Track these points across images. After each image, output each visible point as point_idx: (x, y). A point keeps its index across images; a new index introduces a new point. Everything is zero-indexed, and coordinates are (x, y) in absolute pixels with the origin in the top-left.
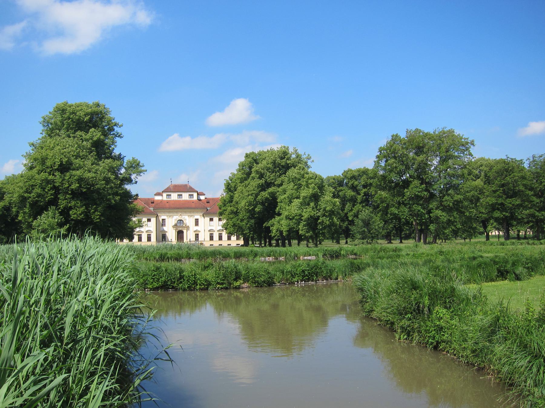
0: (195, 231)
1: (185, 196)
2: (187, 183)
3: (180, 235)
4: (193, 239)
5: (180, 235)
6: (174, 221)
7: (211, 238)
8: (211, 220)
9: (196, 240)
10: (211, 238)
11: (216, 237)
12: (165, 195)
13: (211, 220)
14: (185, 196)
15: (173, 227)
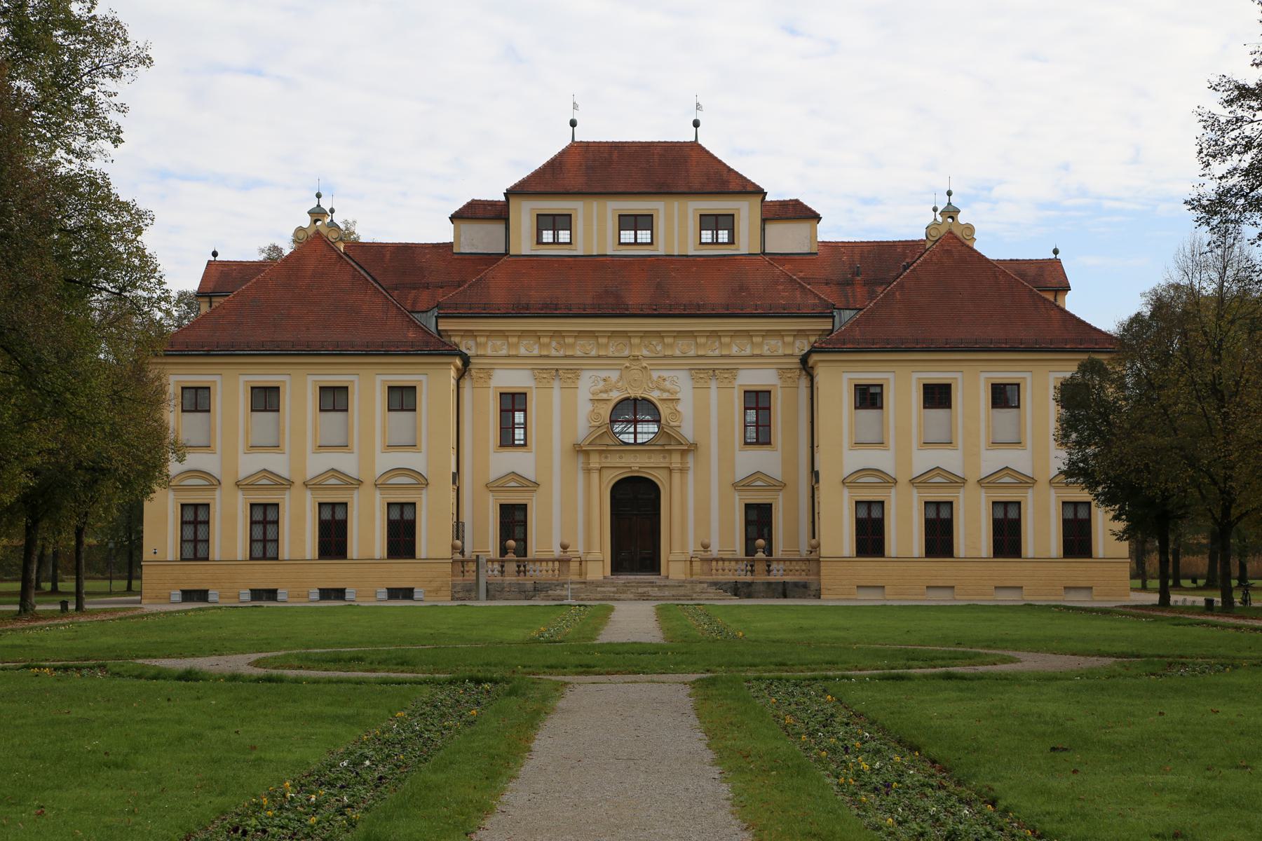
0: (742, 485)
1: (677, 228)
2: (687, 136)
3: (636, 517)
4: (728, 536)
5: (636, 517)
6: (584, 409)
7: (870, 536)
8: (868, 397)
9: (750, 550)
10: (870, 536)
11: (905, 532)
12: (524, 214)
13: (868, 397)
14: (677, 228)
15: (580, 451)
